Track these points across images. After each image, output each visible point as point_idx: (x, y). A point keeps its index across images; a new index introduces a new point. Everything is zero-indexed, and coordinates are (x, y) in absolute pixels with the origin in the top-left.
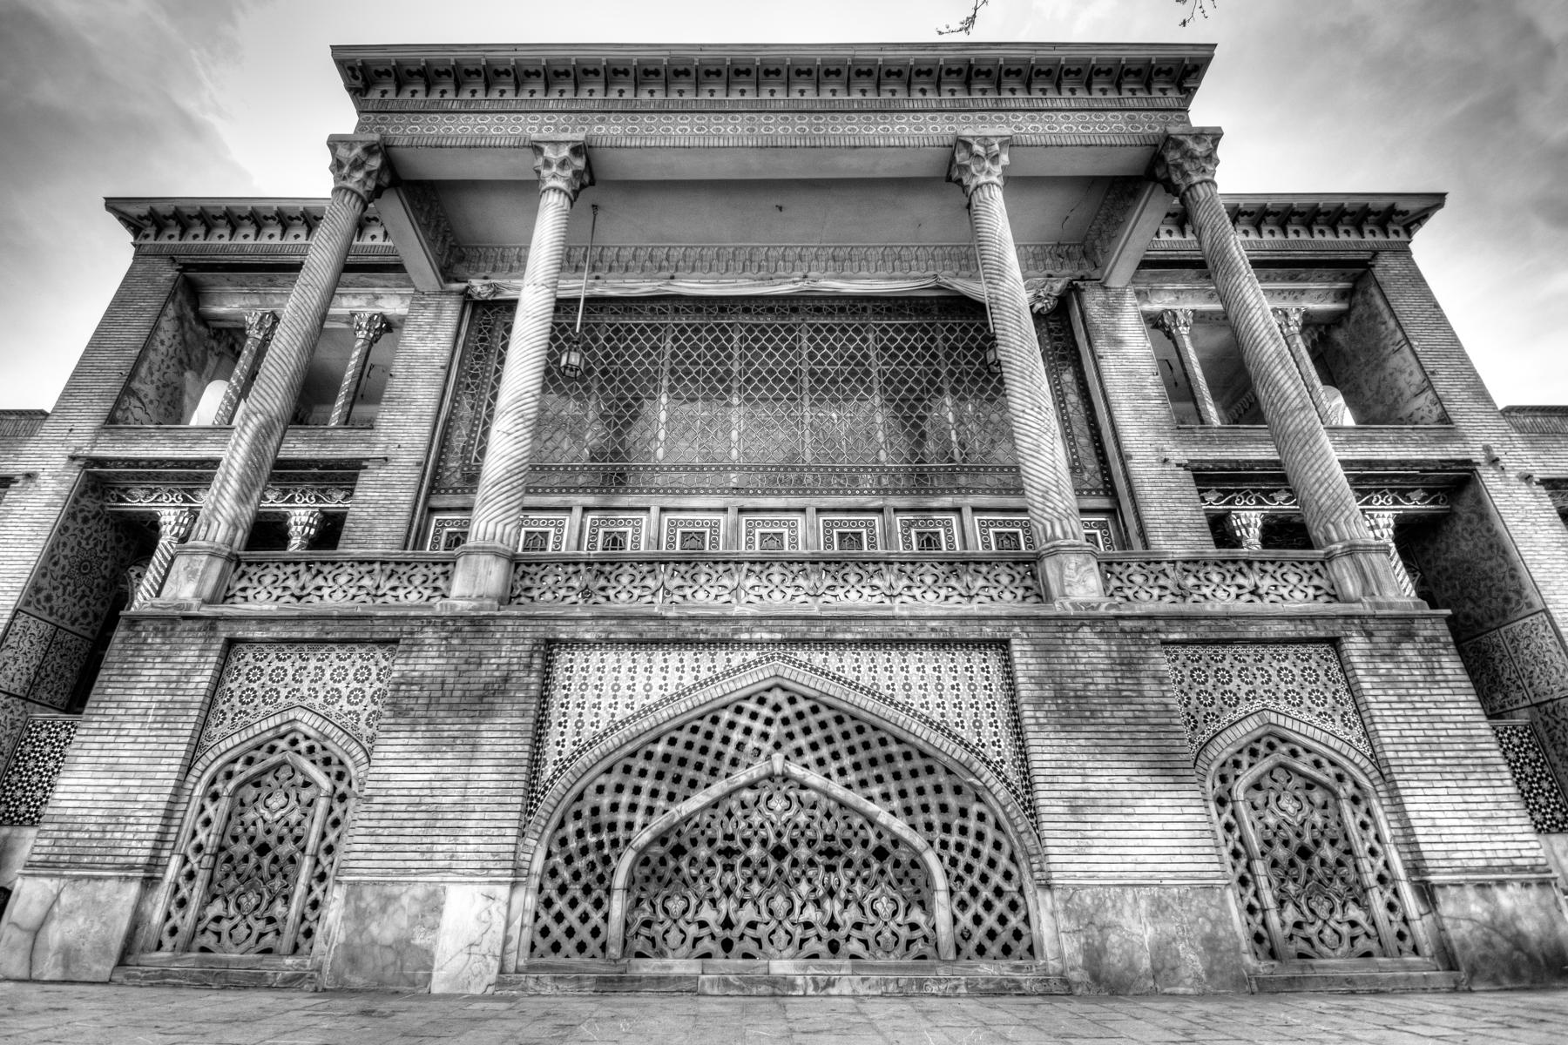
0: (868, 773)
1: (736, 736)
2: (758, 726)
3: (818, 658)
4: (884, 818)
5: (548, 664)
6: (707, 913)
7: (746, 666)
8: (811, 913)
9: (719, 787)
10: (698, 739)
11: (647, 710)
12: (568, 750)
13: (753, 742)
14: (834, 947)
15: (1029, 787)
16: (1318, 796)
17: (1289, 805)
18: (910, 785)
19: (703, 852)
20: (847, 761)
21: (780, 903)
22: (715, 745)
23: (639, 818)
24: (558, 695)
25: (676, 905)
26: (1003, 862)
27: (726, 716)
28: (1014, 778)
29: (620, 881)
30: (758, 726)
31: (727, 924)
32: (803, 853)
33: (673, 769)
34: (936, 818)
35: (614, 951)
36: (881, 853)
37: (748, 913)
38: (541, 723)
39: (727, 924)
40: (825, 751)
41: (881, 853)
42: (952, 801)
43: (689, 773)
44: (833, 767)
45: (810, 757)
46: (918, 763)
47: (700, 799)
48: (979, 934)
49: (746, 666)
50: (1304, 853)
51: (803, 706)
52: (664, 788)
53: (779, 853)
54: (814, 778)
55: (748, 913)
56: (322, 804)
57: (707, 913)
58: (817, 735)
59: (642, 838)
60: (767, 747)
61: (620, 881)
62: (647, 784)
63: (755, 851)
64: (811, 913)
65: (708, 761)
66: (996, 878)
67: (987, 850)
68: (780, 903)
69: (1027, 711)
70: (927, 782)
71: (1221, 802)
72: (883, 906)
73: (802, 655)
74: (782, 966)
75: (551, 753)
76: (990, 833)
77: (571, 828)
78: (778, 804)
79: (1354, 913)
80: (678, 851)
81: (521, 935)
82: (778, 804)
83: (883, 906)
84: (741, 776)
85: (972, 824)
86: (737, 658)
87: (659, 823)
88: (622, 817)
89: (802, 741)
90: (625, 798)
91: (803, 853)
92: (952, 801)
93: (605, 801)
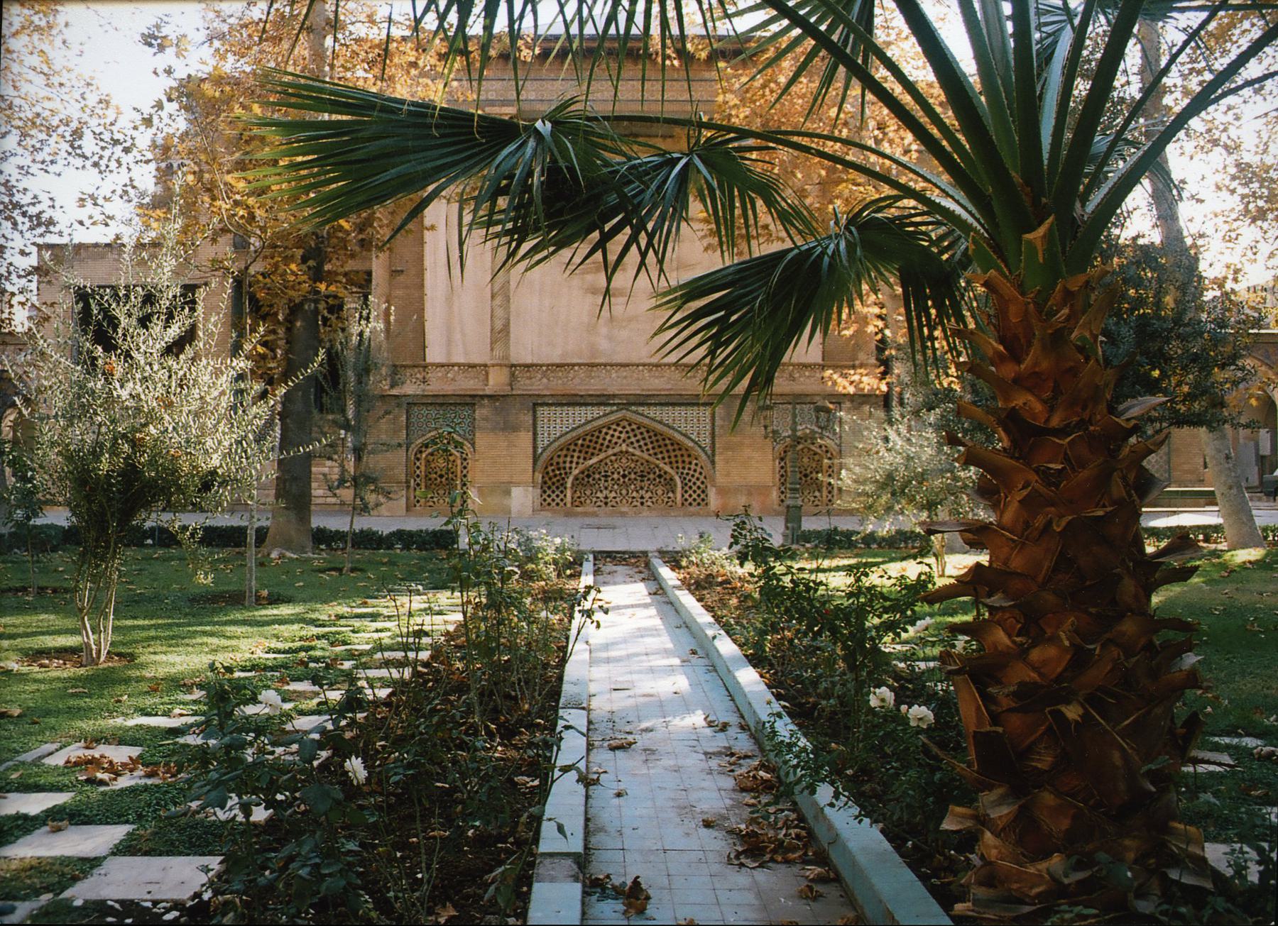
0: (657, 450)
1: (608, 437)
2: (617, 434)
3: (640, 409)
4: (662, 465)
5: (535, 412)
6: (599, 494)
7: (612, 412)
8: (635, 494)
9: (602, 456)
10: (594, 439)
11: (574, 429)
12: (546, 442)
13: (615, 440)
14: (642, 504)
15: (714, 455)
16: (817, 457)
17: (805, 460)
18: (672, 454)
19: (597, 476)
20: (650, 446)
21: (624, 492)
22: (600, 441)
23: (574, 465)
24: (539, 423)
25: (588, 492)
26: (702, 478)
27: (604, 430)
28: (709, 452)
29: (569, 485)
30: (617, 434)
31: (606, 498)
32: (633, 476)
33: (585, 449)
34: (680, 465)
35: (569, 505)
36: (660, 476)
37: (613, 494)
38: (535, 434)
39: (606, 498)
40: (642, 443)
41: (660, 476)
42: (687, 459)
43: (591, 450)
44: (644, 448)
45: (636, 445)
46: (676, 447)
47: (594, 460)
48: (690, 500)
49: (612, 412)
50: (806, 476)
51: (634, 427)
52: (582, 455)
53: (624, 476)
54: (637, 452)
55: (613, 494)
56: (459, 462)
57: (599, 494)
58: (639, 437)
59: (576, 472)
60: (620, 441)
61: (569, 485)
62: (576, 454)
63: (616, 476)
64: (635, 494)
65: (598, 446)
66: (698, 483)
67: (697, 475)
68: (624, 492)
69: (717, 429)
70: (678, 453)
71: (782, 459)
72: (660, 492)
73: (633, 408)
74: (624, 509)
75: (540, 445)
76: (699, 470)
77: (550, 469)
78: (624, 460)
79: (817, 494)
80: (588, 476)
81: (538, 501)
82: (624, 460)
83: (660, 492)
84: (610, 452)
85: (693, 467)
86: (608, 409)
87: (581, 467)
88: (568, 465)
89: (633, 439)
90: (568, 459)
91: (633, 476)
92: (687, 459)
93: (561, 460)
